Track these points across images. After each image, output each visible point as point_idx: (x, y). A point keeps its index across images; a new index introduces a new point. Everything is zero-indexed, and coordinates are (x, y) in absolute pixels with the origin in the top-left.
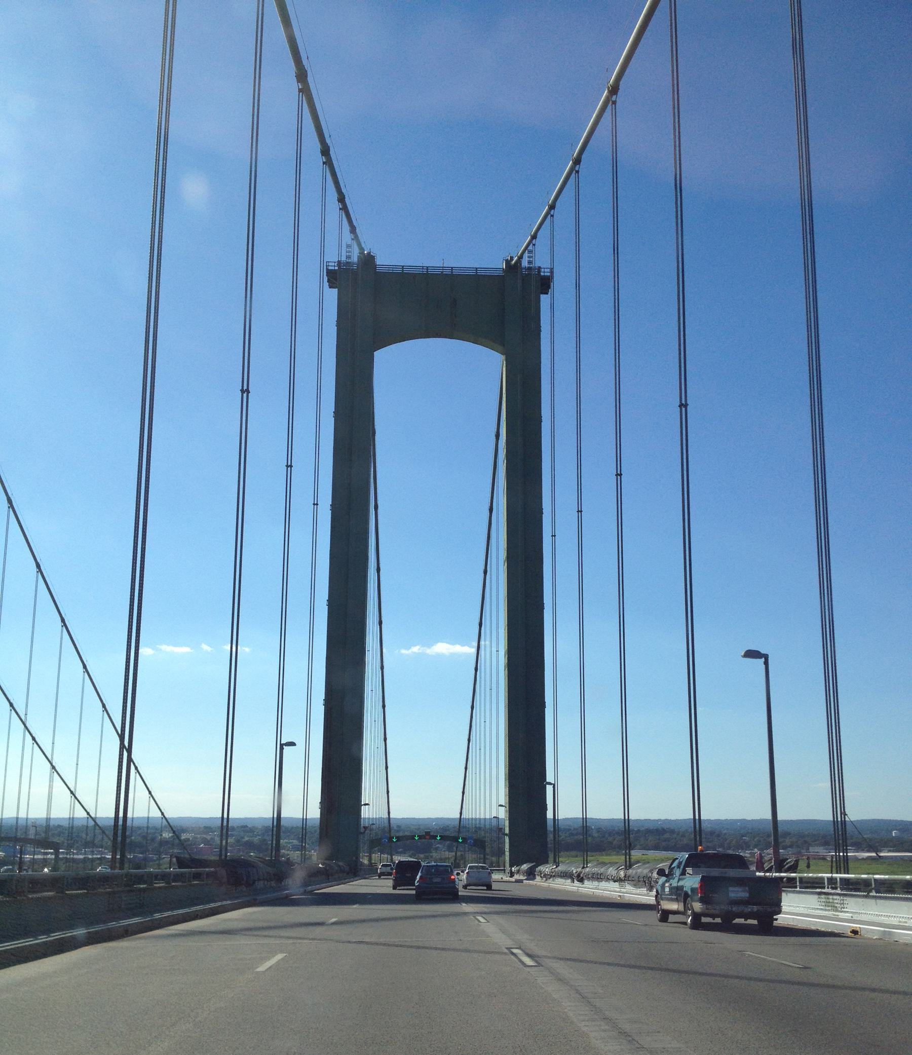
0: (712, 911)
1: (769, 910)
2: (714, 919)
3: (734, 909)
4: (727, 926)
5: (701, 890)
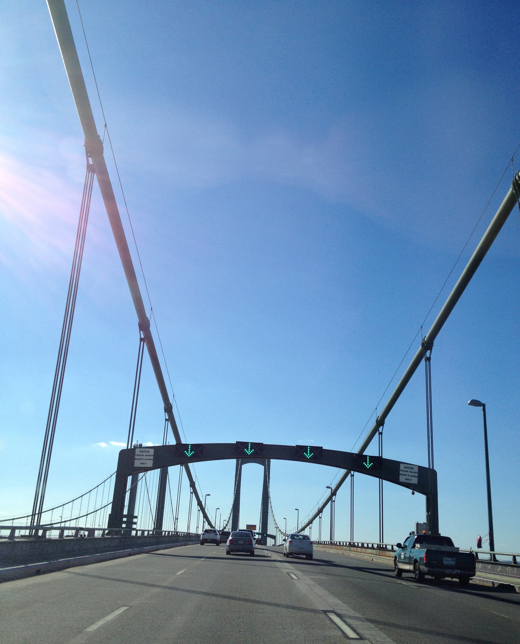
1: (468, 573)
5: (426, 558)
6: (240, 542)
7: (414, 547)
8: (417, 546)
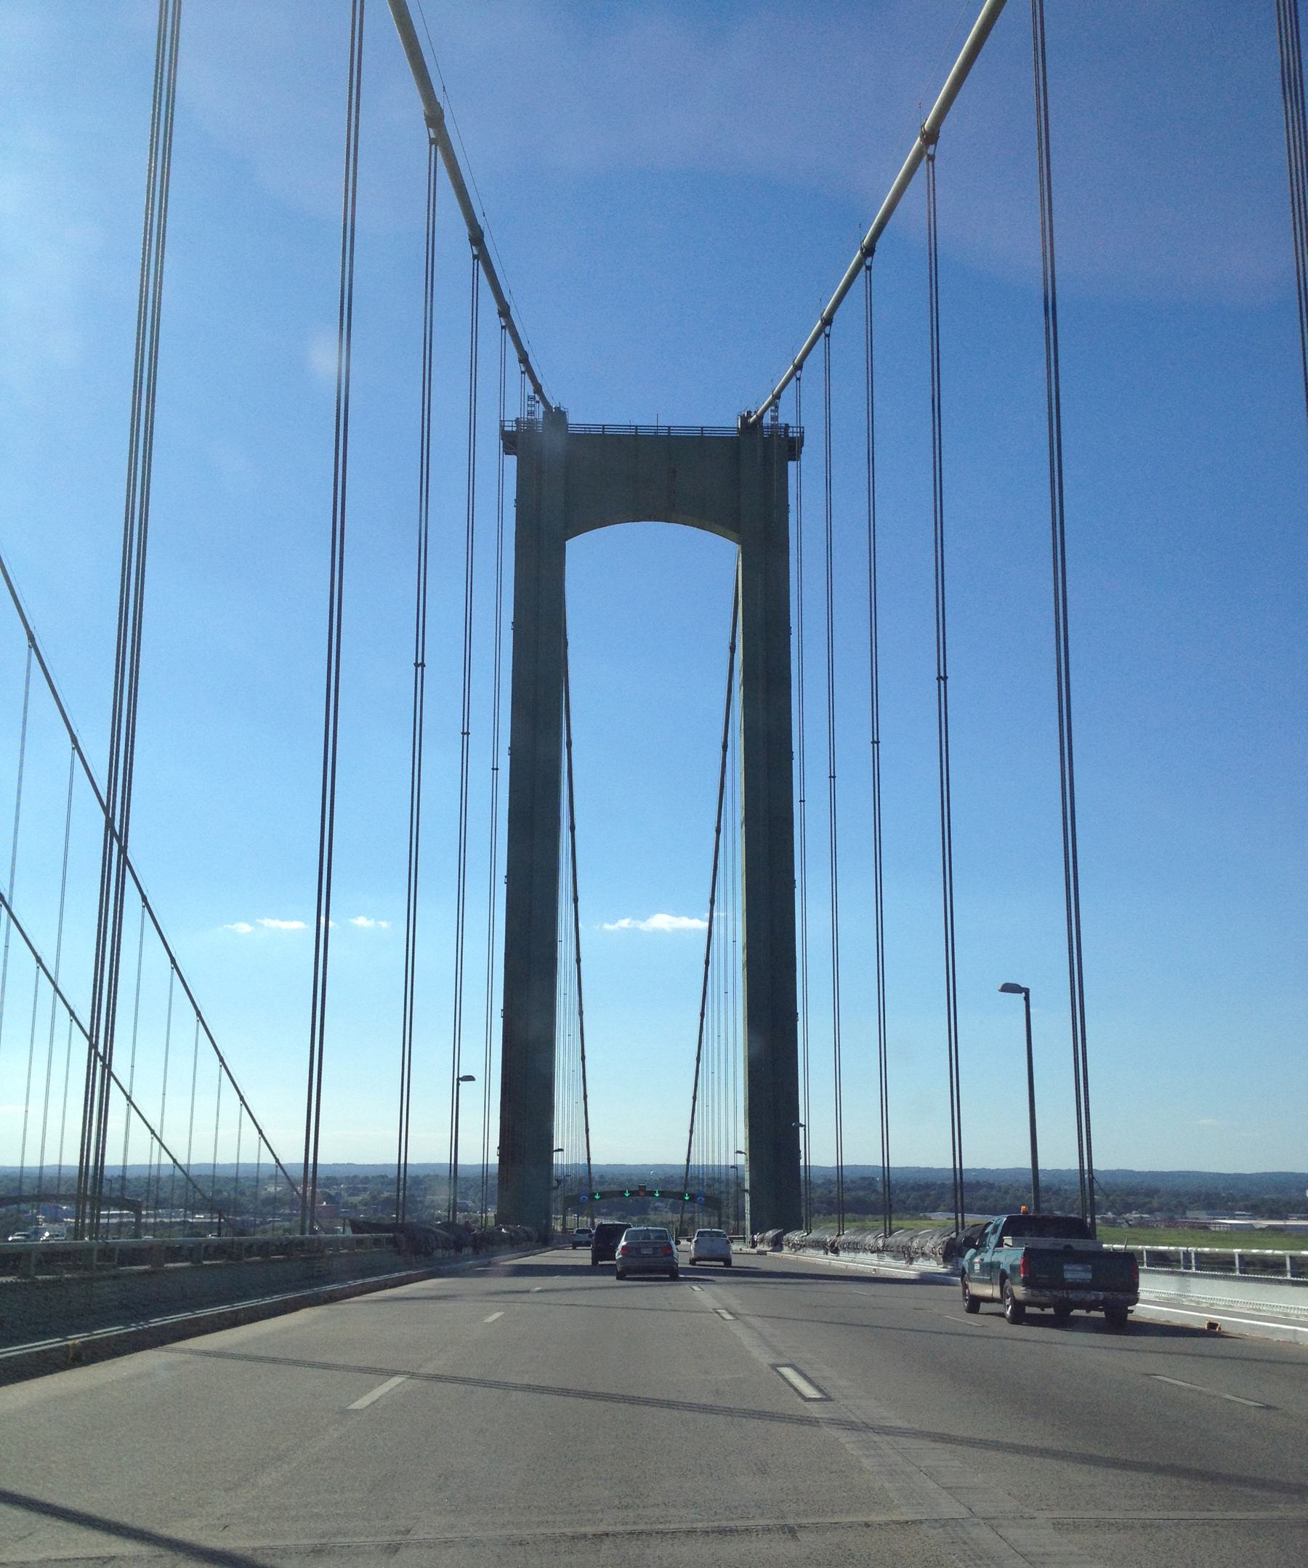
0: (1044, 1300)
1: (1120, 1297)
2: (1043, 1310)
3: (1071, 1296)
4: (1062, 1321)
5: (1024, 1268)
6: (645, 1252)
7: (1000, 1243)
8: (1005, 1241)
